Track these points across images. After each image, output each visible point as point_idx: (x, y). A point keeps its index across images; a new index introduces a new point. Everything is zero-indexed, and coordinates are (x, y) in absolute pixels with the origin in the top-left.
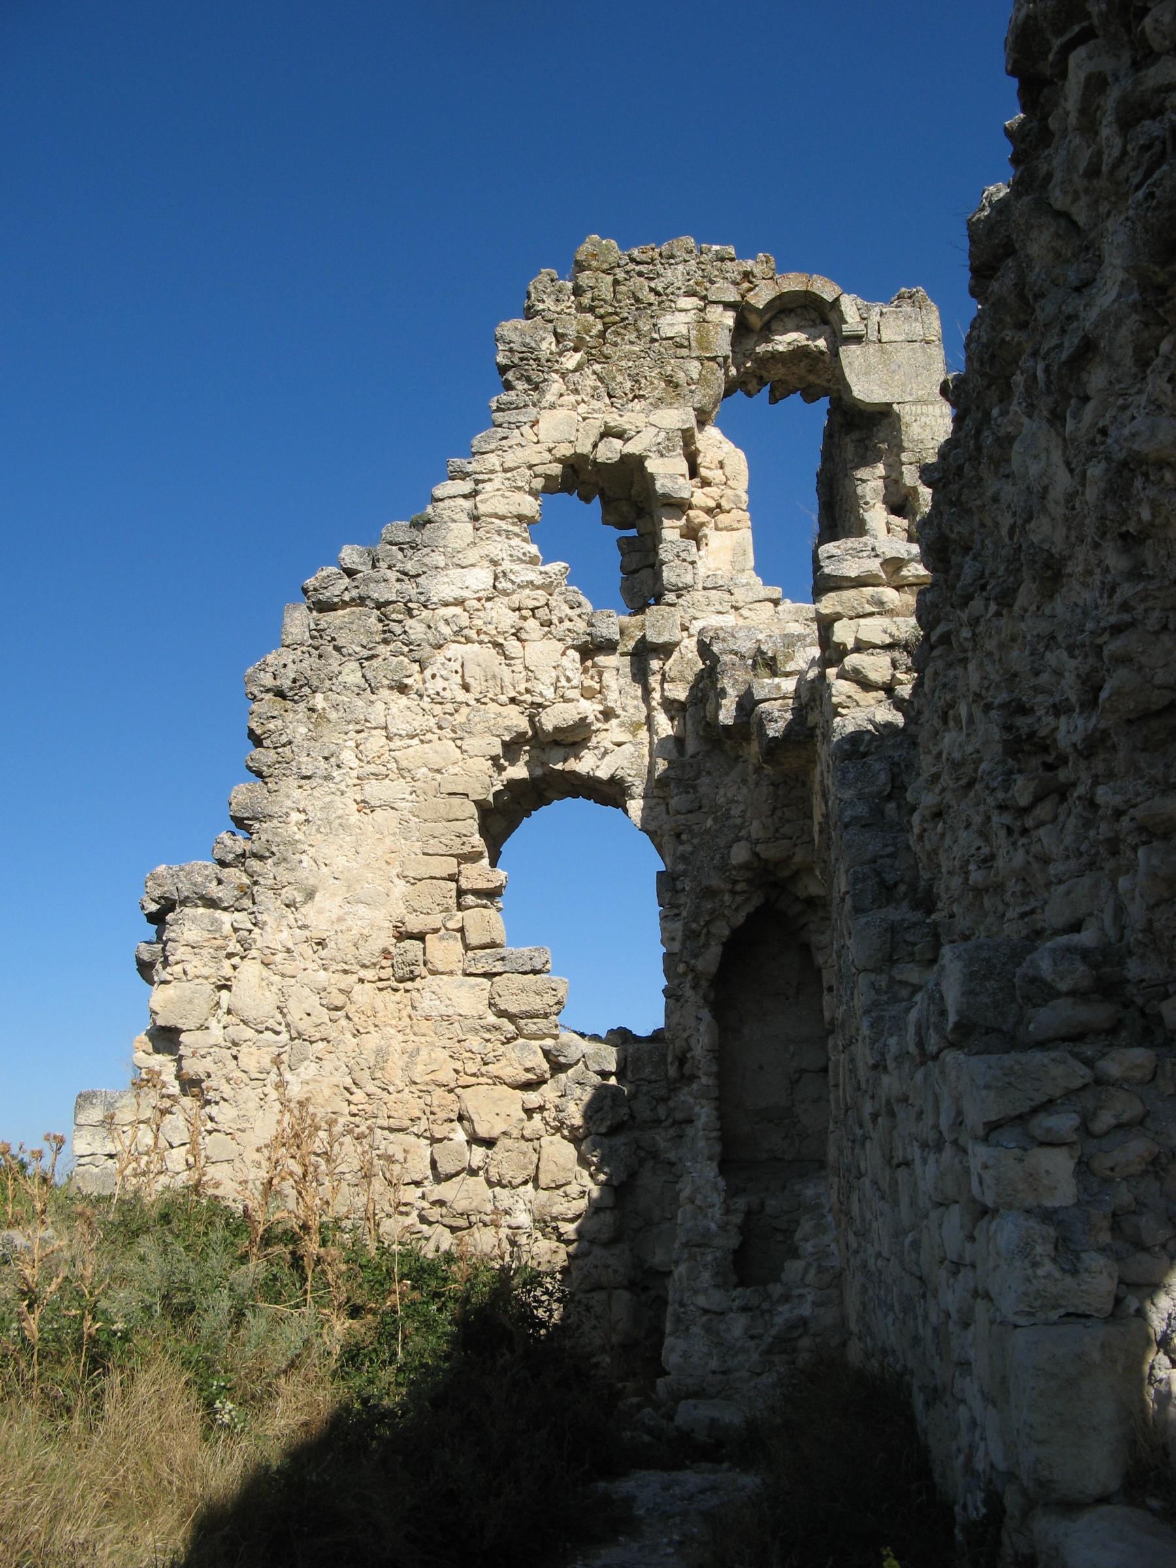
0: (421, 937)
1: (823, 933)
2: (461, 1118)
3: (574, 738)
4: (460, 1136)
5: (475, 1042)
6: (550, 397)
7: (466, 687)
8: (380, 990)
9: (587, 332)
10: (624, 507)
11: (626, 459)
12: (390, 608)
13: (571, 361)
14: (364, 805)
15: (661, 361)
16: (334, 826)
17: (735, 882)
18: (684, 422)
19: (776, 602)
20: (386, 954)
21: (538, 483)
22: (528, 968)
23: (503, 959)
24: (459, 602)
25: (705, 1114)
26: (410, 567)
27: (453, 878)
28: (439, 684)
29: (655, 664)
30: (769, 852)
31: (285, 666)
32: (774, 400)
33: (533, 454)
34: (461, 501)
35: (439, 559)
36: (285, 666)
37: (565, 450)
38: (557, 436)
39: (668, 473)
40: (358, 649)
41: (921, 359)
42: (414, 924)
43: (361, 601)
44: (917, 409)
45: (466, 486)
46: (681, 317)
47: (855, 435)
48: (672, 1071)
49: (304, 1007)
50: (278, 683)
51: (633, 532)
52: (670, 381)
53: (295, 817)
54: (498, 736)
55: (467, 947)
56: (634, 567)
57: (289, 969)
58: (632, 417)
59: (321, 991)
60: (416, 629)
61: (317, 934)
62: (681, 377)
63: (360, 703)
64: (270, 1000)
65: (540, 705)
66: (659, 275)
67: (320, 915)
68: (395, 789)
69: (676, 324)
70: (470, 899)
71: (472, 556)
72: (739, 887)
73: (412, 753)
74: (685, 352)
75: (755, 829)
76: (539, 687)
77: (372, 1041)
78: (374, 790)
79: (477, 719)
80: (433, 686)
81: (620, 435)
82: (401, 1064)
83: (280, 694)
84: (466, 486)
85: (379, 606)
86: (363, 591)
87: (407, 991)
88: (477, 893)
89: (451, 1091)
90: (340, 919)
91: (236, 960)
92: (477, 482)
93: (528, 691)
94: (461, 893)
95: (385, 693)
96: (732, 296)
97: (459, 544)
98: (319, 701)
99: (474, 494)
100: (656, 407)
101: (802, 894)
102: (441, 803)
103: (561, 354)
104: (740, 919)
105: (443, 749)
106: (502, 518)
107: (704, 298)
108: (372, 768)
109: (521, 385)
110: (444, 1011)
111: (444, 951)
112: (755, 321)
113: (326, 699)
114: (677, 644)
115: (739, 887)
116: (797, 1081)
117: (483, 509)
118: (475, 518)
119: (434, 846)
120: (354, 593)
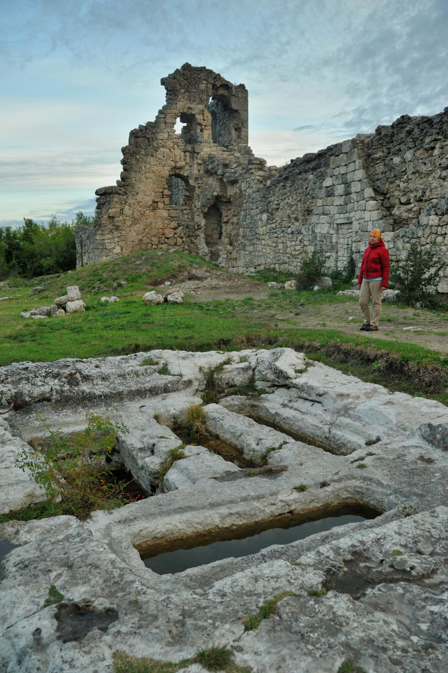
0: (157, 202)
2: (164, 234)
3: (181, 168)
4: (163, 237)
5: (166, 221)
6: (179, 99)
7: (164, 157)
11: (191, 114)
13: (182, 91)
14: (146, 178)
15: (199, 95)
16: (140, 181)
20: (151, 205)
24: (162, 140)
25: (202, 235)
26: (153, 131)
27: (162, 192)
28: (160, 156)
29: (196, 156)
30: (220, 194)
35: (159, 130)
37: (181, 111)
42: (156, 200)
43: (144, 137)
44: (242, 112)
45: (164, 116)
46: (203, 85)
51: (185, 124)
52: (200, 98)
53: (133, 179)
55: (165, 205)
57: (134, 207)
60: (155, 145)
62: (203, 99)
64: (131, 213)
67: (140, 197)
68: (152, 175)
70: (165, 196)
71: (165, 131)
75: (218, 189)
77: (149, 220)
78: (148, 175)
80: (158, 156)
81: (191, 109)
85: (148, 139)
94: (163, 195)
95: (150, 156)
96: (213, 82)
97: (163, 128)
98: (138, 157)
99: (165, 118)
102: (160, 178)
105: (160, 168)
109: (173, 95)
111: (161, 205)
117: (167, 121)
118: (165, 123)
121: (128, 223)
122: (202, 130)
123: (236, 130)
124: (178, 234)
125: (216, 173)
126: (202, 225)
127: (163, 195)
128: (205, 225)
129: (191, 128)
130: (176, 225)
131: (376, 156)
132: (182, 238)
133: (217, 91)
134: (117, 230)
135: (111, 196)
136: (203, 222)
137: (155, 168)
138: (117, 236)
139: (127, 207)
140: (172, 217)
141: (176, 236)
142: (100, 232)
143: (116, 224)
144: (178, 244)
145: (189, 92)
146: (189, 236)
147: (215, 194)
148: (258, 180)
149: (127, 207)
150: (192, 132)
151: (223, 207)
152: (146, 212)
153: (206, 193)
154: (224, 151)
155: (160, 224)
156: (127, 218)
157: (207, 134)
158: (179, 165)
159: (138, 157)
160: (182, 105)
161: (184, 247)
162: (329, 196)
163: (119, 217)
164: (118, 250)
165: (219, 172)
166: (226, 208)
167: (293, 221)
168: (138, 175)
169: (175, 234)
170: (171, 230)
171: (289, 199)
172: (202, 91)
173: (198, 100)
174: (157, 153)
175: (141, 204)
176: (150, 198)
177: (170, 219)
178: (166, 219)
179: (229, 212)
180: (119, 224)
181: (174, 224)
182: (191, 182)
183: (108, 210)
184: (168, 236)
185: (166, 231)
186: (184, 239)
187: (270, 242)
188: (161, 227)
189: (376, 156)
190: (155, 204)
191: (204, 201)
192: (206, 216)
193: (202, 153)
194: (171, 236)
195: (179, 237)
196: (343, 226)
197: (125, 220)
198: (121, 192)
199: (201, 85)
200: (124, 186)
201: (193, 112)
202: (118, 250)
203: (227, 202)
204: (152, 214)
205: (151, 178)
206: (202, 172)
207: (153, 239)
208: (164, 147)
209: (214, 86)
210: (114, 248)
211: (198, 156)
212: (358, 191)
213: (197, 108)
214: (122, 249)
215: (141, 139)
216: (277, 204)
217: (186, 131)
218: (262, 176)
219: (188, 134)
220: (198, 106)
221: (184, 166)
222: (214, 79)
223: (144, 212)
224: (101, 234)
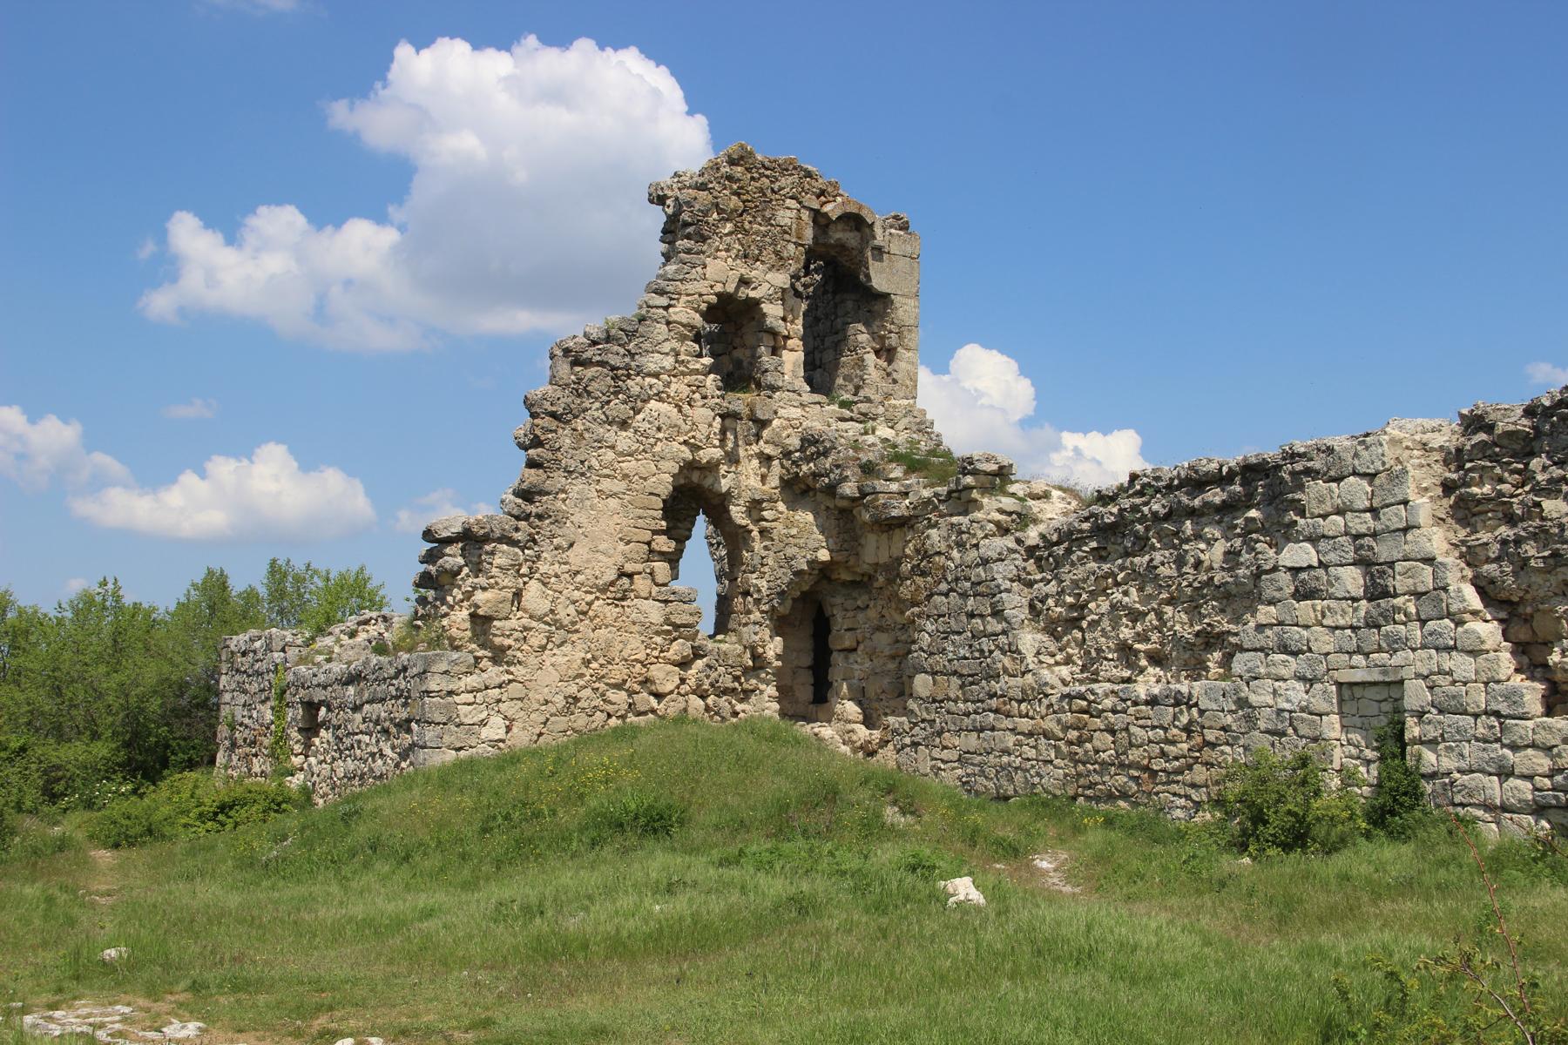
0: (630, 576)
5: (658, 639)
20: (612, 584)
21: (704, 306)
25: (771, 690)
27: (649, 543)
33: (702, 287)
37: (719, 288)
39: (773, 311)
42: (629, 568)
43: (602, 364)
45: (664, 301)
49: (566, 613)
52: (777, 253)
58: (756, 272)
59: (574, 602)
61: (574, 568)
62: (785, 254)
67: (576, 557)
68: (619, 486)
69: (785, 217)
71: (666, 347)
73: (629, 465)
76: (698, 435)
78: (606, 485)
83: (553, 415)
84: (664, 301)
85: (613, 368)
90: (588, 561)
94: (651, 551)
106: (684, 326)
111: (641, 584)
118: (668, 323)
119: (641, 523)
121: (536, 640)
122: (775, 351)
123: (877, 353)
124: (692, 682)
125: (831, 490)
126: (770, 654)
128: (778, 657)
129: (737, 341)
130: (688, 651)
131: (1475, 490)
132: (703, 697)
134: (495, 660)
135: (488, 548)
136: (773, 647)
137: (629, 465)
138: (498, 681)
139: (534, 587)
140: (677, 627)
141: (684, 688)
142: (443, 667)
143: (497, 640)
146: (726, 691)
148: (998, 524)
149: (534, 587)
150: (738, 354)
151: (838, 600)
152: (594, 607)
153: (790, 551)
154: (843, 419)
155: (635, 646)
156: (534, 624)
157: (793, 359)
158: (705, 455)
159: (580, 428)
160: (719, 271)
162: (1306, 598)
163: (507, 618)
164: (495, 729)
165: (849, 489)
166: (849, 604)
167: (1143, 662)
168: (577, 487)
169: (683, 681)
171: (1126, 593)
173: (768, 255)
174: (640, 417)
175: (580, 578)
176: (610, 561)
177: (668, 633)
178: (658, 633)
179: (861, 616)
180: (507, 642)
181: (679, 648)
182: (737, 513)
183: (468, 595)
184: (661, 689)
185: (657, 672)
186: (710, 700)
187: (1050, 724)
188: (641, 656)
189: (1475, 490)
190: (625, 580)
191: (786, 577)
192: (780, 625)
193: (776, 423)
194: (669, 687)
195: (694, 692)
196: (1358, 692)
197: (526, 629)
198: (517, 536)
200: (527, 517)
201: (752, 294)
202: (495, 729)
203: (853, 582)
205: (613, 495)
206: (774, 481)
207: (612, 695)
208: (661, 400)
209: (817, 215)
210: (483, 723)
211: (766, 433)
212: (1421, 589)
213: (768, 282)
214: (509, 729)
215: (592, 372)
216: (1072, 607)
218: (1010, 514)
219: (725, 359)
220: (769, 276)
221: (718, 463)
223: (590, 604)
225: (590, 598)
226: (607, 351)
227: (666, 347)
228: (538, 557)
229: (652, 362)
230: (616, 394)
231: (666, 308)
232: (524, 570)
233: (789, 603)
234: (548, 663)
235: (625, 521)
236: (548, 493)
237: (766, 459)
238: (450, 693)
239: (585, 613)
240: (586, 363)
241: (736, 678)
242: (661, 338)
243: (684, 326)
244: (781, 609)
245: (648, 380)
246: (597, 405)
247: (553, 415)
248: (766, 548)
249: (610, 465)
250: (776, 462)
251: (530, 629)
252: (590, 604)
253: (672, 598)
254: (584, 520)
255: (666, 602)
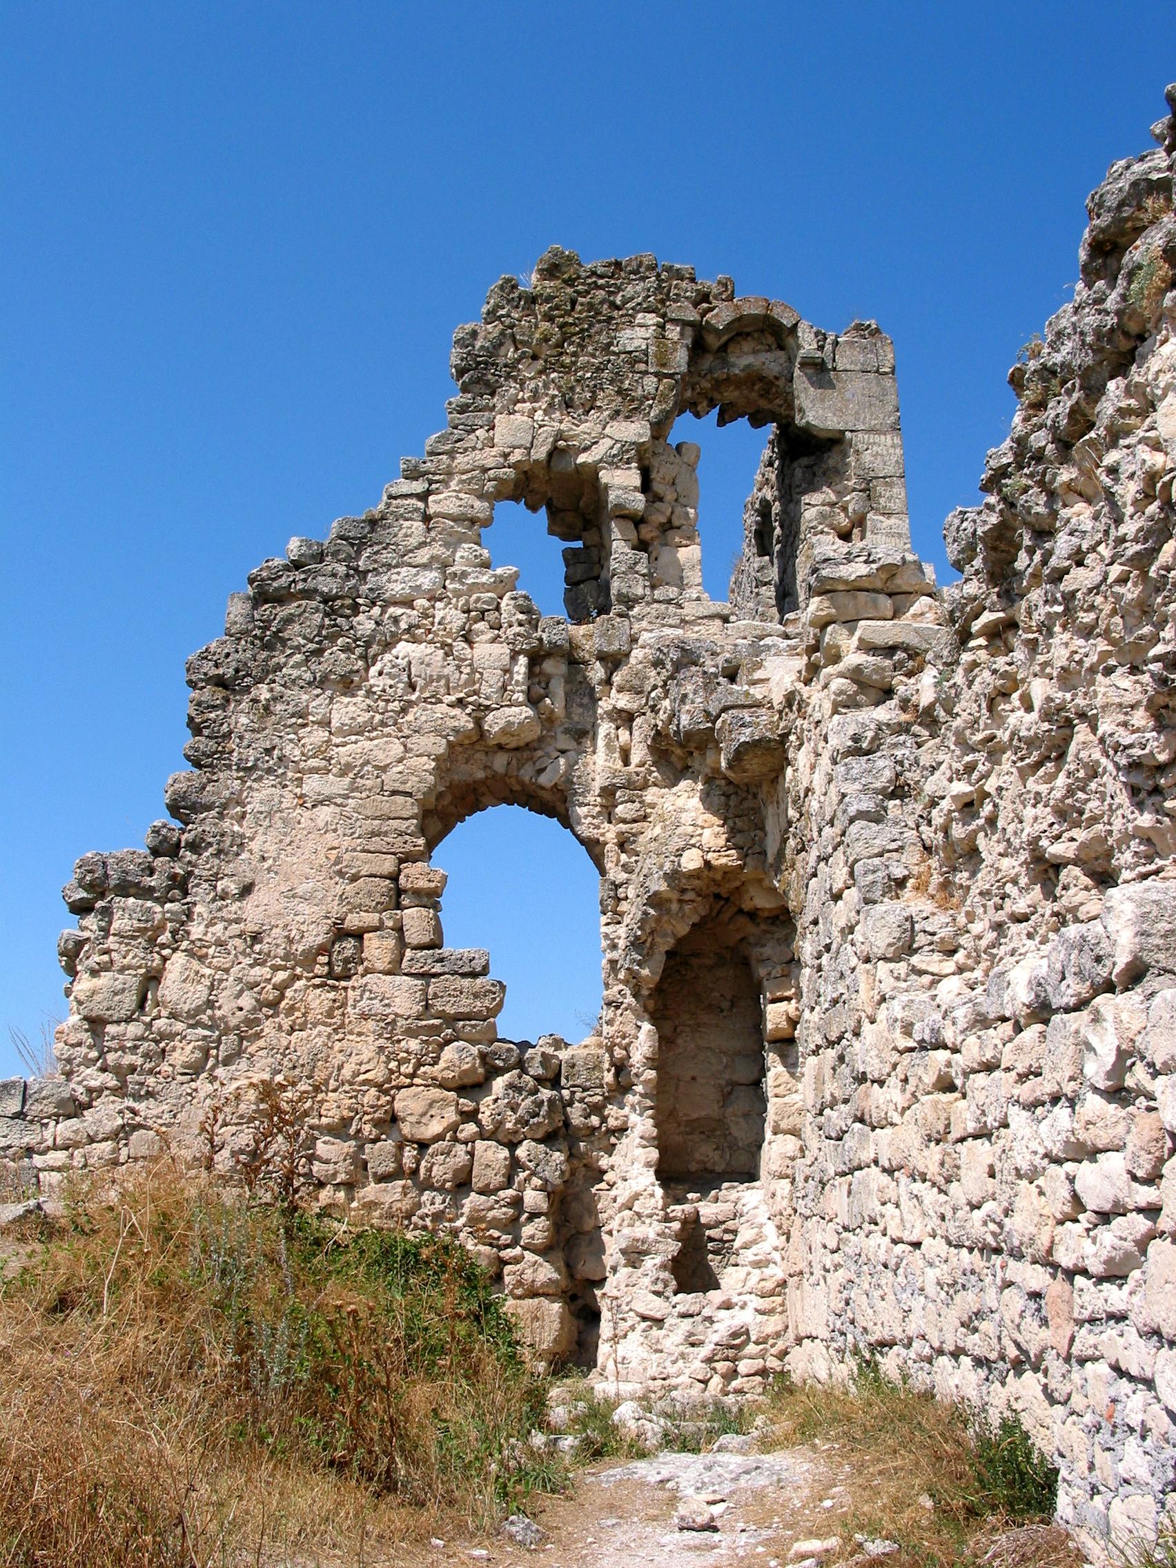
0: (358, 935)
1: (763, 946)
7: (412, 686)
8: (316, 986)
9: (546, 340)
10: (570, 517)
12: (339, 602)
17: (683, 891)
18: (640, 435)
19: (726, 620)
20: (324, 949)
22: (466, 969)
23: (441, 960)
25: (642, 1125)
27: (394, 877)
31: (228, 655)
32: (722, 422)
33: (488, 457)
34: (414, 501)
36: (228, 655)
37: (517, 456)
38: (510, 440)
40: (303, 642)
41: (875, 390)
42: (354, 921)
43: (308, 594)
45: (419, 486)
46: (641, 332)
47: (805, 461)
48: (609, 1077)
50: (221, 671)
51: (579, 544)
54: (445, 737)
56: (578, 577)
61: (252, 927)
63: (305, 697)
65: (487, 707)
66: (619, 289)
71: (423, 556)
72: (687, 897)
74: (642, 367)
78: (312, 785)
79: (423, 718)
82: (336, 1062)
84: (419, 486)
86: (311, 584)
87: (345, 989)
88: (417, 893)
89: (386, 1092)
91: (166, 952)
92: (431, 482)
93: (476, 693)
96: (692, 315)
100: (612, 418)
101: (747, 906)
103: (519, 361)
104: (683, 929)
106: (455, 519)
107: (663, 316)
108: (313, 763)
110: (381, 1010)
112: (713, 341)
113: (271, 690)
114: (628, 655)
115: (687, 897)
116: (730, 1093)
118: (427, 518)
120: (300, 586)
127: (399, 892)
128: (651, 1062)
133: (725, 363)
141: (471, 1128)
144: (477, 1182)
145: (566, 369)
147: (691, 861)
158: (494, 722)
161: (517, 1203)
170: (436, 1093)
172: (634, 359)
174: (373, 671)
176: (319, 911)
177: (435, 1030)
178: (411, 1033)
181: (457, 1057)
185: (407, 1103)
188: (378, 1074)
194: (435, 1127)
198: (152, 882)
199: (628, 333)
201: (582, 458)
204: (319, 1000)
217: (579, 571)
222: (696, 304)
223: (282, 988)
224: (20, 1115)
225: (281, 976)
226: (316, 573)
227: (423, 556)
228: (189, 915)
229: (397, 583)
230: (333, 638)
231: (423, 497)
232: (165, 938)
233: (659, 959)
234: (202, 1094)
235: (346, 842)
236: (208, 808)
237: (625, 718)
238: (29, 1151)
239: (274, 1005)
240: (280, 598)
241: (597, 1109)
242: (413, 542)
243: (455, 519)
244: (645, 972)
245: (391, 610)
246: (298, 657)
247: (220, 682)
248: (626, 868)
249: (320, 751)
250: (638, 721)
251: (172, 1036)
252: (282, 988)
253: (438, 968)
254: (272, 849)
255: (426, 976)
